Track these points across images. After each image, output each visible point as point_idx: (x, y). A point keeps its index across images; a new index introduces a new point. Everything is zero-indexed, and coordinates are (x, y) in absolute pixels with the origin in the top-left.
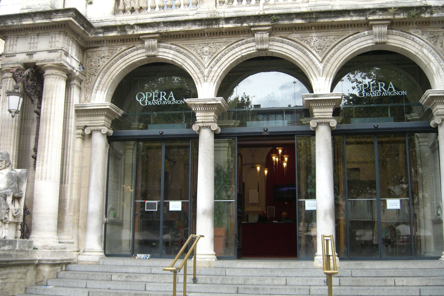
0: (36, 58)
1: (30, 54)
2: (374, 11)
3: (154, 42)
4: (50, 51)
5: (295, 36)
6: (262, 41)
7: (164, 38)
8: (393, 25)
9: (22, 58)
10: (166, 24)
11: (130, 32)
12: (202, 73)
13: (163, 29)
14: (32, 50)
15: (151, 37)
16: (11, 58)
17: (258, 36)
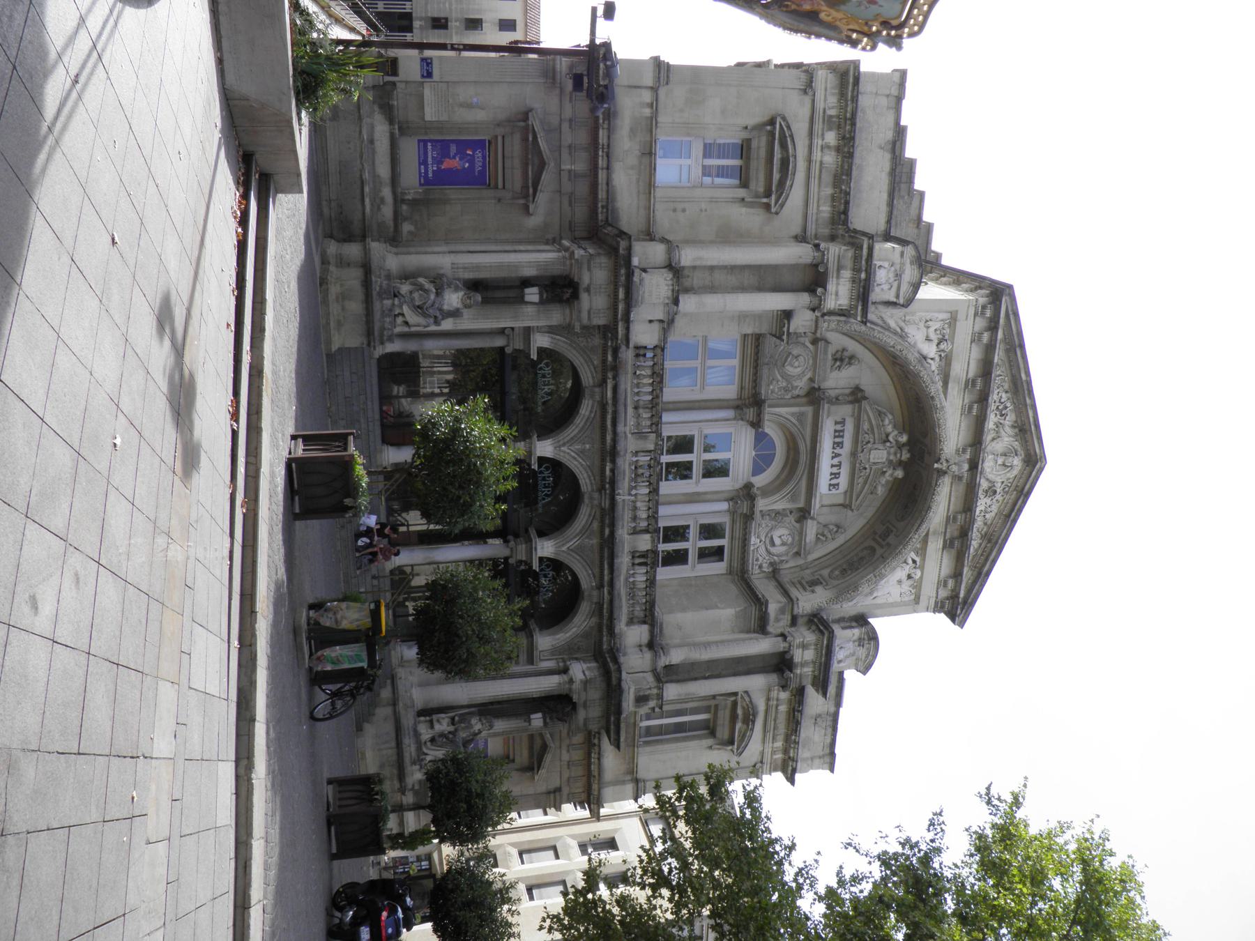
0: (584, 296)
1: (588, 290)
2: (611, 593)
3: (598, 398)
4: (589, 312)
5: (596, 525)
6: (591, 498)
7: (603, 406)
8: (600, 606)
9: (586, 279)
10: (615, 413)
11: (610, 375)
12: (564, 445)
13: (610, 409)
14: (592, 291)
15: (603, 395)
16: (585, 266)
17: (596, 495)
